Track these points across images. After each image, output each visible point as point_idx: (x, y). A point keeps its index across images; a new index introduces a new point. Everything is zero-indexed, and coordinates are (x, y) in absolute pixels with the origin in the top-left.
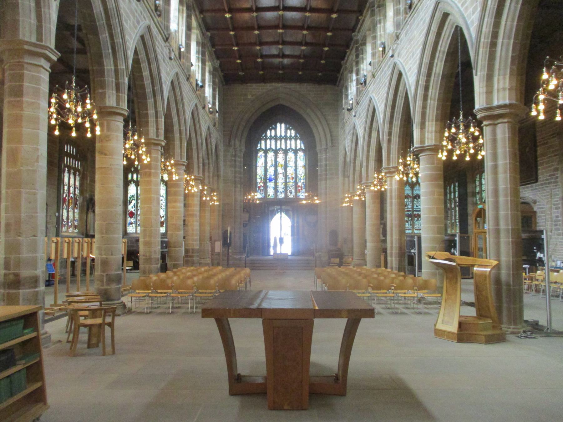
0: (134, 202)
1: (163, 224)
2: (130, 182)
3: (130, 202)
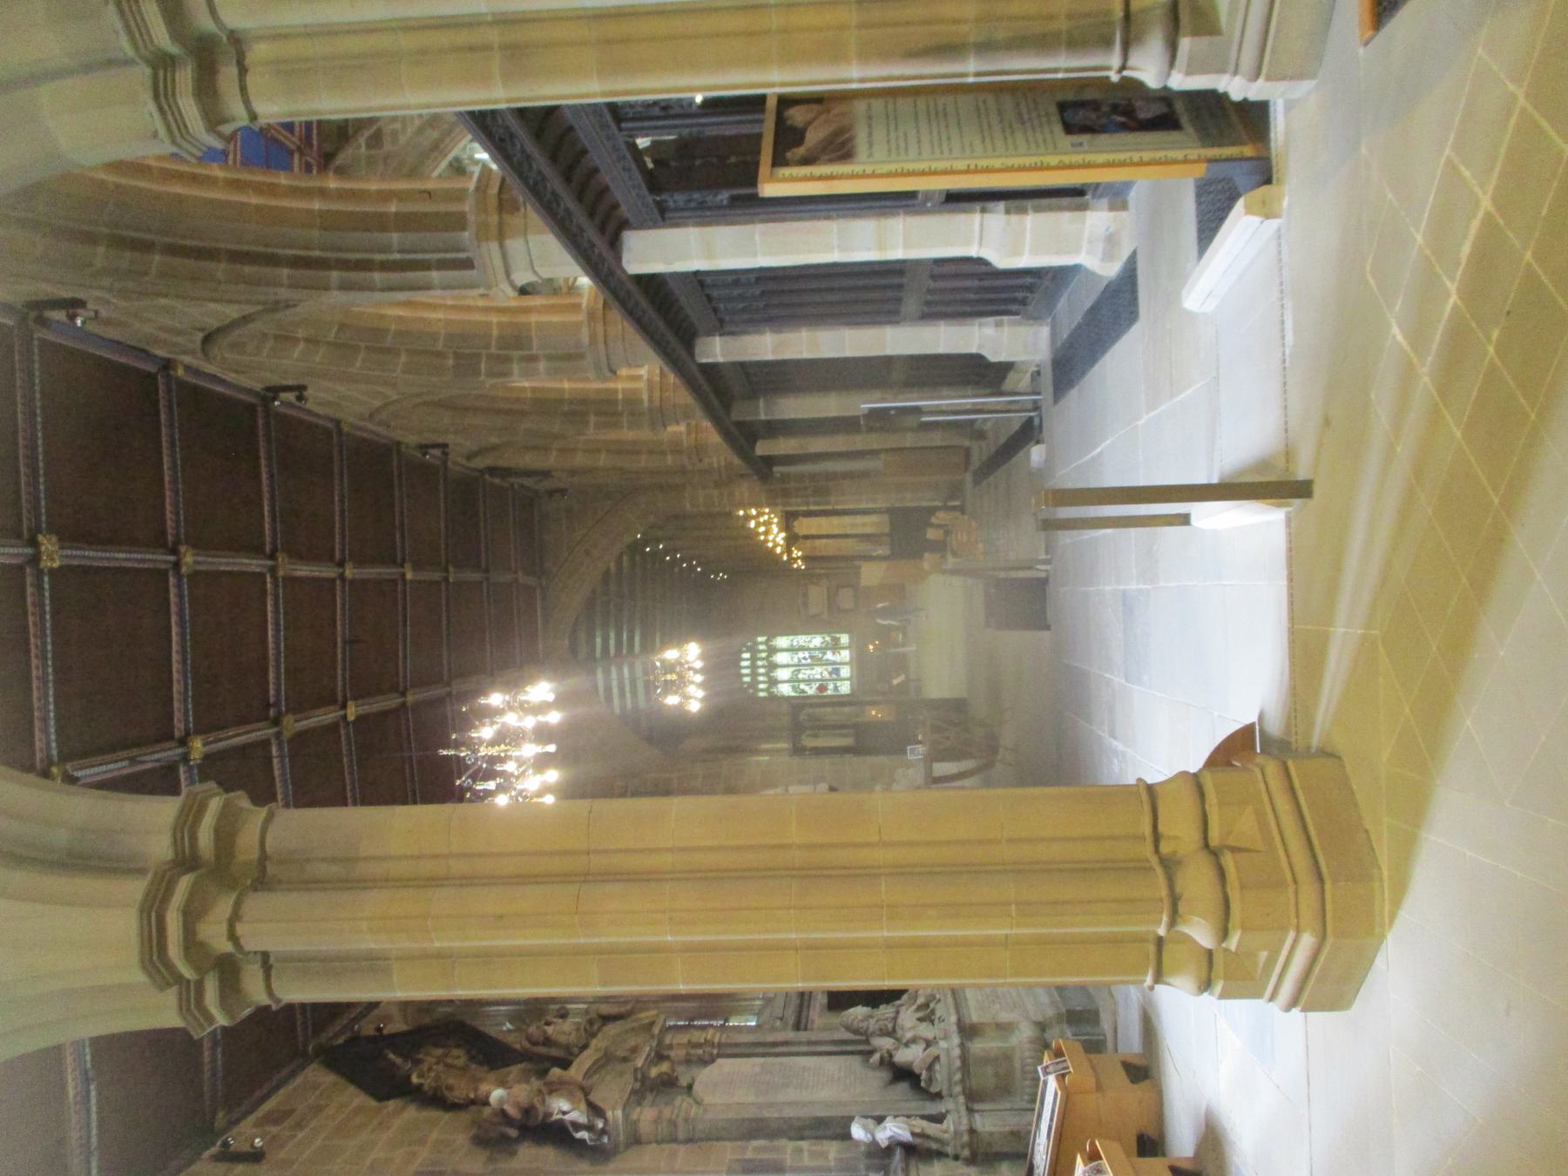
0: (802, 686)
2: (771, 693)
3: (803, 691)
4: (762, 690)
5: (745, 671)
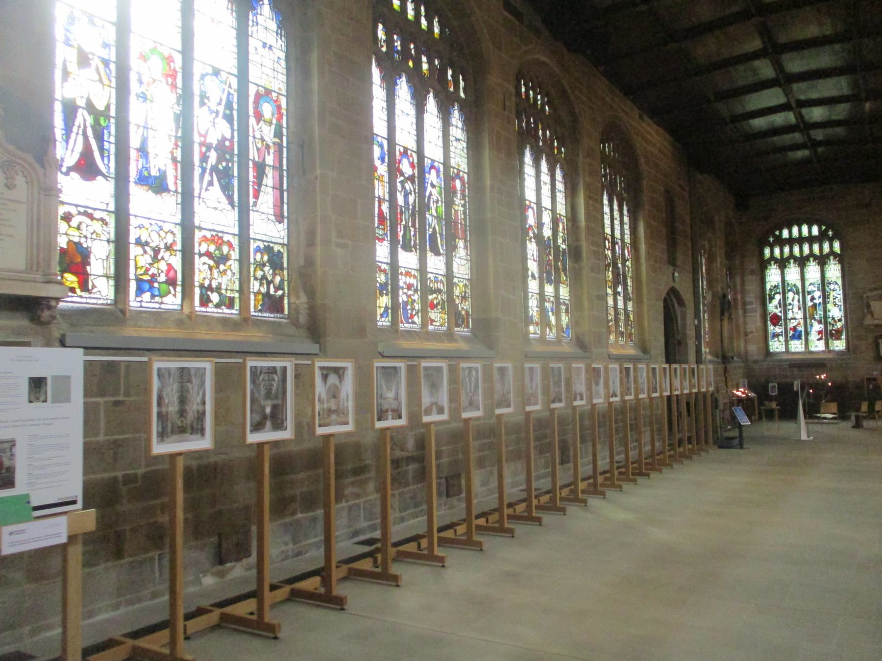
0: (778, 297)
1: (841, 335)
2: (768, 262)
3: (772, 298)
4: (772, 252)
5: (795, 230)
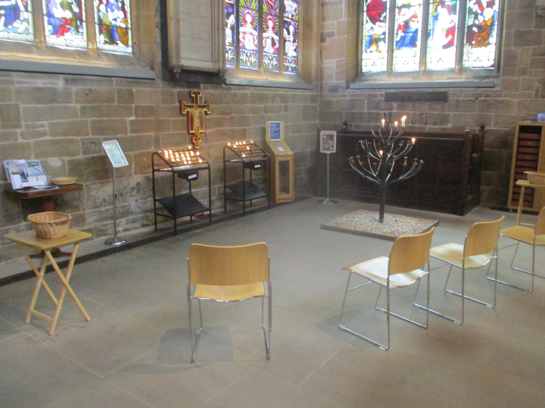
1: (489, 35)
